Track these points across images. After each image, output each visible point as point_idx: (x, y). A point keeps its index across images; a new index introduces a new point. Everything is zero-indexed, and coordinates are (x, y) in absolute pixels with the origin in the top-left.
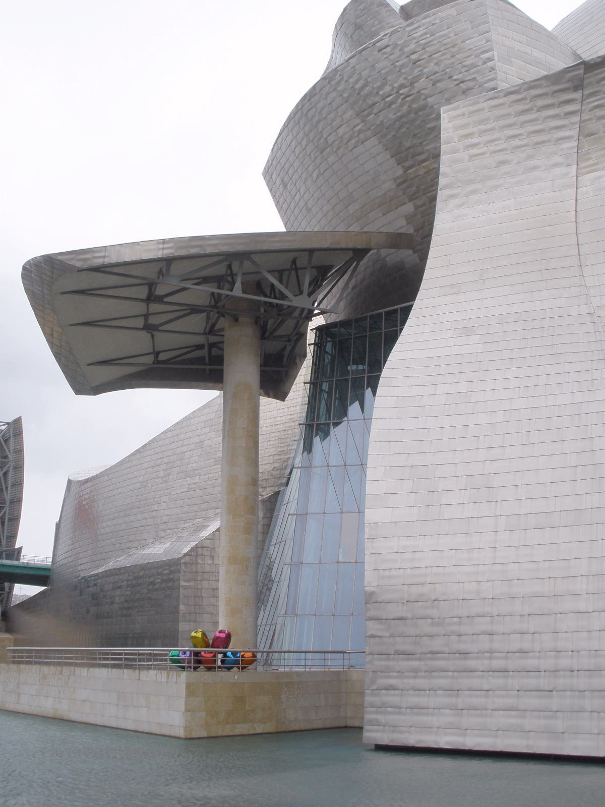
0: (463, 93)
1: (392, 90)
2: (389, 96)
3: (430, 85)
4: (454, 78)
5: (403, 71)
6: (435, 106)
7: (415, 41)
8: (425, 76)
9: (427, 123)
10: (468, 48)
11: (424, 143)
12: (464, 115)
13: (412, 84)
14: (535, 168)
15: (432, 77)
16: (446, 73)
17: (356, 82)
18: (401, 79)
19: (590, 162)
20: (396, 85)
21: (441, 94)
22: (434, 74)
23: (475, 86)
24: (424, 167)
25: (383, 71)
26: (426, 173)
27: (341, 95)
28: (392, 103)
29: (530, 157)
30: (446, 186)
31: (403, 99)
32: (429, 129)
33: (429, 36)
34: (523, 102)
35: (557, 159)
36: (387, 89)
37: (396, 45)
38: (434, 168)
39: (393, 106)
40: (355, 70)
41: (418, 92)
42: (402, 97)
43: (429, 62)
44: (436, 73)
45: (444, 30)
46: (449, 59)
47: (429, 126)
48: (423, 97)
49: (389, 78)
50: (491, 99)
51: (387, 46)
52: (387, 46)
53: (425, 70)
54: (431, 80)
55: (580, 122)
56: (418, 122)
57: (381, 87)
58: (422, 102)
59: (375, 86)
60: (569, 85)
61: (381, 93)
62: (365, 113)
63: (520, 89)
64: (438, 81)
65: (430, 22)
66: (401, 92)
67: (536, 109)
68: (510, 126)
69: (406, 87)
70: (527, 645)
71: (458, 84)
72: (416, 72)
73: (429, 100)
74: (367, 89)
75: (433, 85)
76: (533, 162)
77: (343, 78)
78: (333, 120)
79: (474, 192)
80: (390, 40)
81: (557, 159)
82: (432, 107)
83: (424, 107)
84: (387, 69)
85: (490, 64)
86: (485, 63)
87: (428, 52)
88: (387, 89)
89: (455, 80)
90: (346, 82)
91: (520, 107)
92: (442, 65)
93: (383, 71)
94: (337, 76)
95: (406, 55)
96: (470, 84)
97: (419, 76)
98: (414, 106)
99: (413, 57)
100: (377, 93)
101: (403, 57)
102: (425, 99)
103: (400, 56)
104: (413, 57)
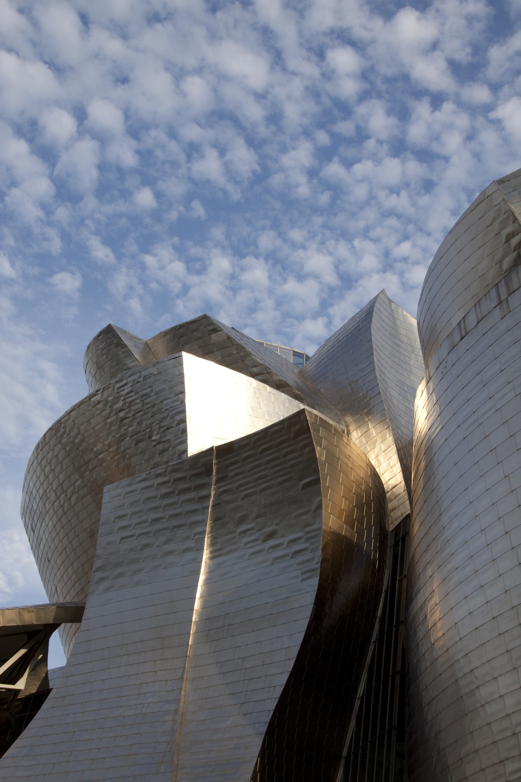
0: (159, 454)
2: (100, 454)
3: (133, 445)
4: (154, 438)
5: (112, 428)
6: (137, 467)
7: (122, 398)
8: (130, 435)
10: (165, 408)
12: (120, 495)
14: (170, 553)
15: (135, 437)
16: (146, 434)
17: (76, 436)
18: (110, 437)
20: (106, 442)
22: (137, 434)
23: (169, 447)
25: (97, 428)
27: (65, 448)
28: (104, 460)
29: (168, 541)
30: (98, 569)
33: (133, 394)
34: (167, 485)
36: (100, 446)
37: (107, 402)
40: (75, 424)
43: (133, 421)
45: (146, 389)
46: (149, 419)
49: (101, 435)
51: (99, 403)
52: (99, 403)
54: (134, 439)
57: (95, 444)
59: (90, 442)
61: (95, 449)
62: (83, 469)
63: (166, 471)
65: (134, 380)
67: (177, 492)
68: (155, 508)
73: (133, 460)
74: (84, 445)
76: (170, 547)
77: (65, 430)
78: (59, 474)
79: (120, 575)
80: (102, 396)
82: (134, 467)
84: (100, 426)
85: (182, 426)
86: (178, 424)
87: (132, 411)
88: (100, 446)
90: (68, 435)
91: (164, 490)
92: (144, 425)
93: (97, 428)
94: (61, 429)
99: (122, 414)
100: (92, 449)
101: (112, 414)
103: (110, 413)
104: (122, 414)
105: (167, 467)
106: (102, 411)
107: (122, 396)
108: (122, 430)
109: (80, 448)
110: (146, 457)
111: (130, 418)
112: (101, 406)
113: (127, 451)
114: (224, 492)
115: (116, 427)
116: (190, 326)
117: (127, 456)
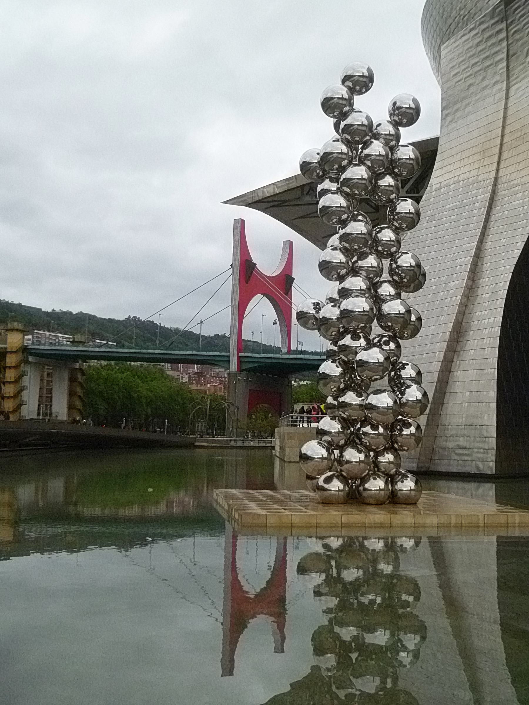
1: (456, 12)
12: (451, 51)
13: (465, 6)
19: (515, 77)
20: (458, 8)
29: (483, 79)
31: (463, 19)
35: (497, 78)
39: (459, 25)
42: (462, 17)
48: (472, 16)
50: (463, 35)
55: (508, 46)
57: (451, 13)
63: (475, 26)
68: (473, 56)
76: (485, 83)
79: (457, 110)
81: (497, 78)
105: (476, 22)
109: (452, 15)
114: (515, 32)
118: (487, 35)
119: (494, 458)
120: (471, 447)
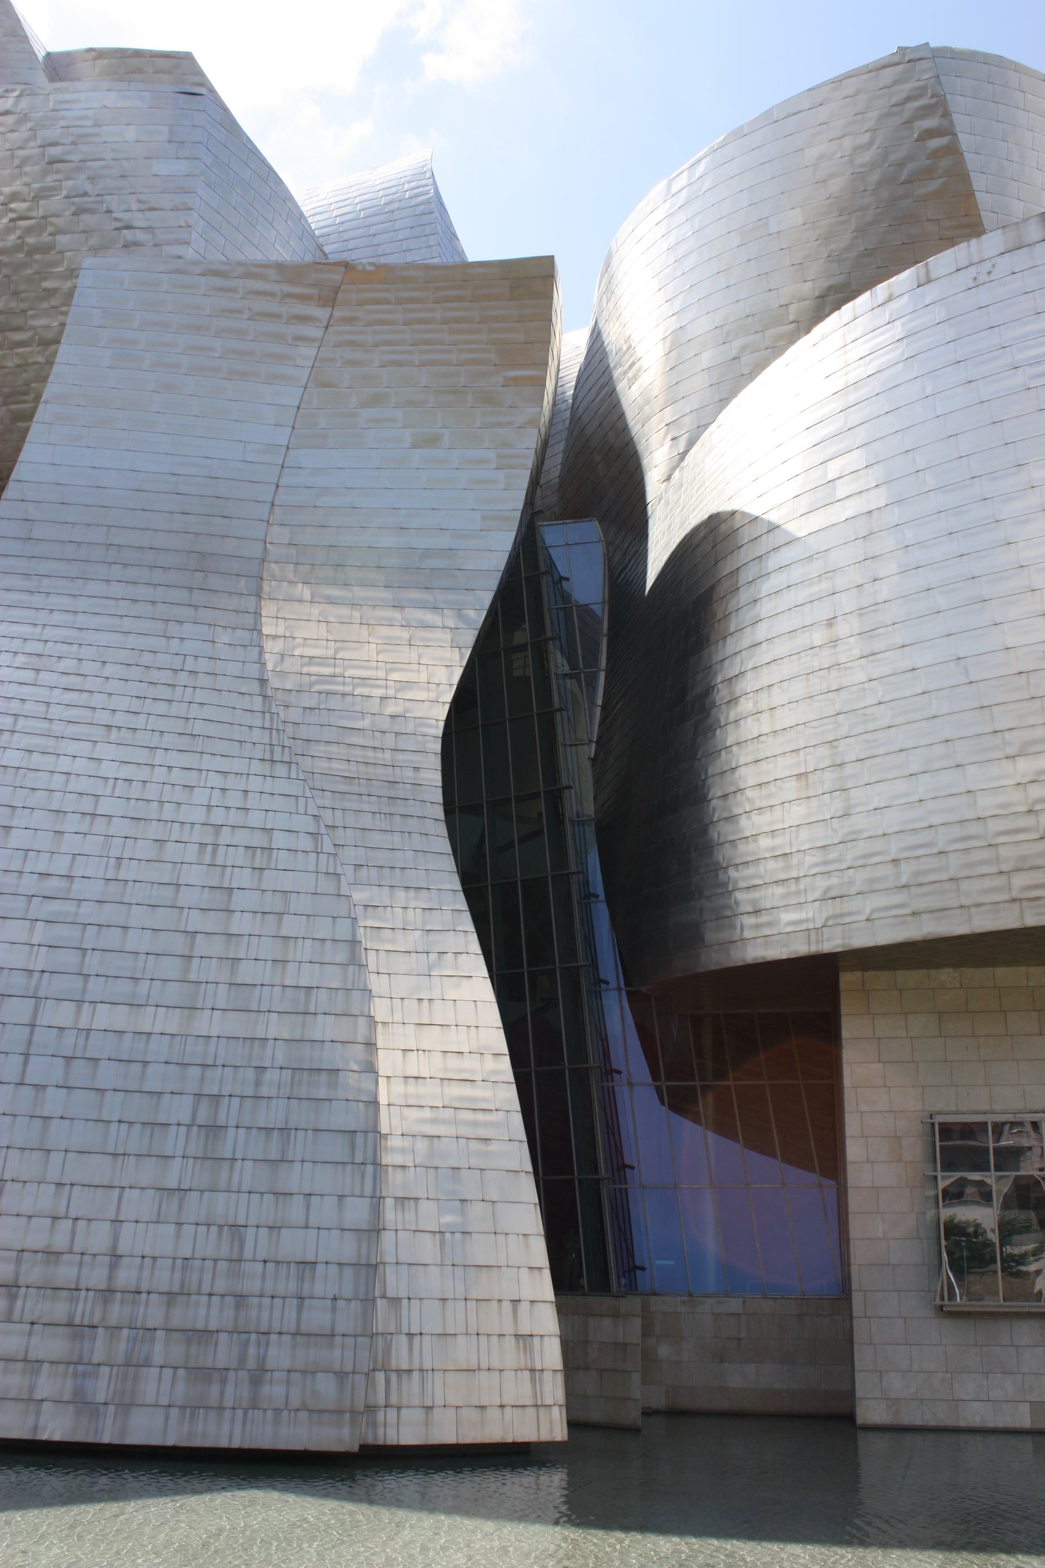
0: (125, 246)
3: (68, 213)
5: (27, 169)
6: (69, 254)
7: (63, 123)
8: (64, 193)
9: (45, 279)
11: (30, 313)
13: (36, 198)
15: (77, 200)
18: (18, 182)
21: (84, 235)
24: (17, 354)
26: (19, 366)
31: (12, 220)
32: (45, 290)
38: (35, 363)
41: (44, 217)
42: (12, 215)
44: (85, 194)
47: (48, 284)
48: (50, 229)
53: (70, 183)
54: (74, 204)
56: (29, 271)
58: (45, 238)
60: (314, 291)
64: (85, 211)
66: (13, 206)
69: (24, 201)
70: (60, 1241)
71: (117, 229)
72: (49, 180)
75: (74, 214)
80: (16, 104)
82: (61, 252)
83: (46, 249)
89: (116, 219)
95: (39, 142)
96: (140, 236)
97: (52, 189)
98: (30, 240)
101: (32, 144)
102: (52, 234)
103: (27, 141)
104: (55, 151)
106: (12, 131)
107: (63, 118)
108: (49, 178)
110: (92, 242)
111: (71, 165)
112: (10, 120)
113: (53, 220)
115: (36, 168)
116: (157, 60)
117: (50, 229)
118: (261, 305)
119: (560, 1396)
120: (496, 1364)
